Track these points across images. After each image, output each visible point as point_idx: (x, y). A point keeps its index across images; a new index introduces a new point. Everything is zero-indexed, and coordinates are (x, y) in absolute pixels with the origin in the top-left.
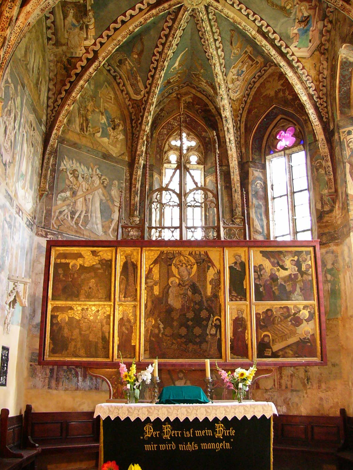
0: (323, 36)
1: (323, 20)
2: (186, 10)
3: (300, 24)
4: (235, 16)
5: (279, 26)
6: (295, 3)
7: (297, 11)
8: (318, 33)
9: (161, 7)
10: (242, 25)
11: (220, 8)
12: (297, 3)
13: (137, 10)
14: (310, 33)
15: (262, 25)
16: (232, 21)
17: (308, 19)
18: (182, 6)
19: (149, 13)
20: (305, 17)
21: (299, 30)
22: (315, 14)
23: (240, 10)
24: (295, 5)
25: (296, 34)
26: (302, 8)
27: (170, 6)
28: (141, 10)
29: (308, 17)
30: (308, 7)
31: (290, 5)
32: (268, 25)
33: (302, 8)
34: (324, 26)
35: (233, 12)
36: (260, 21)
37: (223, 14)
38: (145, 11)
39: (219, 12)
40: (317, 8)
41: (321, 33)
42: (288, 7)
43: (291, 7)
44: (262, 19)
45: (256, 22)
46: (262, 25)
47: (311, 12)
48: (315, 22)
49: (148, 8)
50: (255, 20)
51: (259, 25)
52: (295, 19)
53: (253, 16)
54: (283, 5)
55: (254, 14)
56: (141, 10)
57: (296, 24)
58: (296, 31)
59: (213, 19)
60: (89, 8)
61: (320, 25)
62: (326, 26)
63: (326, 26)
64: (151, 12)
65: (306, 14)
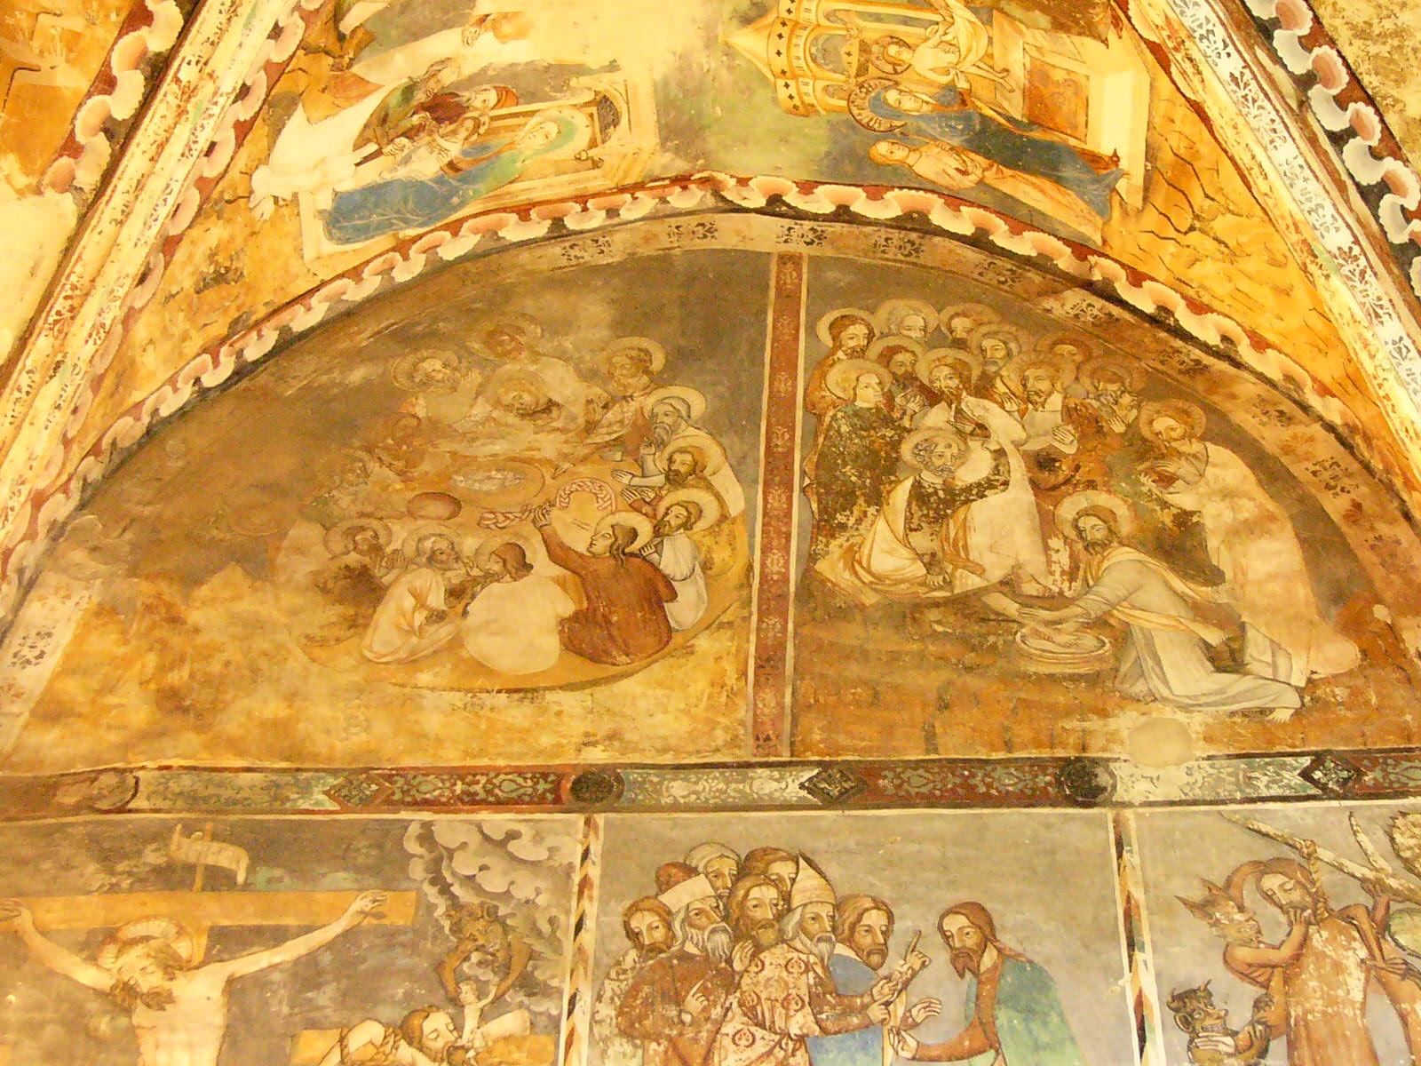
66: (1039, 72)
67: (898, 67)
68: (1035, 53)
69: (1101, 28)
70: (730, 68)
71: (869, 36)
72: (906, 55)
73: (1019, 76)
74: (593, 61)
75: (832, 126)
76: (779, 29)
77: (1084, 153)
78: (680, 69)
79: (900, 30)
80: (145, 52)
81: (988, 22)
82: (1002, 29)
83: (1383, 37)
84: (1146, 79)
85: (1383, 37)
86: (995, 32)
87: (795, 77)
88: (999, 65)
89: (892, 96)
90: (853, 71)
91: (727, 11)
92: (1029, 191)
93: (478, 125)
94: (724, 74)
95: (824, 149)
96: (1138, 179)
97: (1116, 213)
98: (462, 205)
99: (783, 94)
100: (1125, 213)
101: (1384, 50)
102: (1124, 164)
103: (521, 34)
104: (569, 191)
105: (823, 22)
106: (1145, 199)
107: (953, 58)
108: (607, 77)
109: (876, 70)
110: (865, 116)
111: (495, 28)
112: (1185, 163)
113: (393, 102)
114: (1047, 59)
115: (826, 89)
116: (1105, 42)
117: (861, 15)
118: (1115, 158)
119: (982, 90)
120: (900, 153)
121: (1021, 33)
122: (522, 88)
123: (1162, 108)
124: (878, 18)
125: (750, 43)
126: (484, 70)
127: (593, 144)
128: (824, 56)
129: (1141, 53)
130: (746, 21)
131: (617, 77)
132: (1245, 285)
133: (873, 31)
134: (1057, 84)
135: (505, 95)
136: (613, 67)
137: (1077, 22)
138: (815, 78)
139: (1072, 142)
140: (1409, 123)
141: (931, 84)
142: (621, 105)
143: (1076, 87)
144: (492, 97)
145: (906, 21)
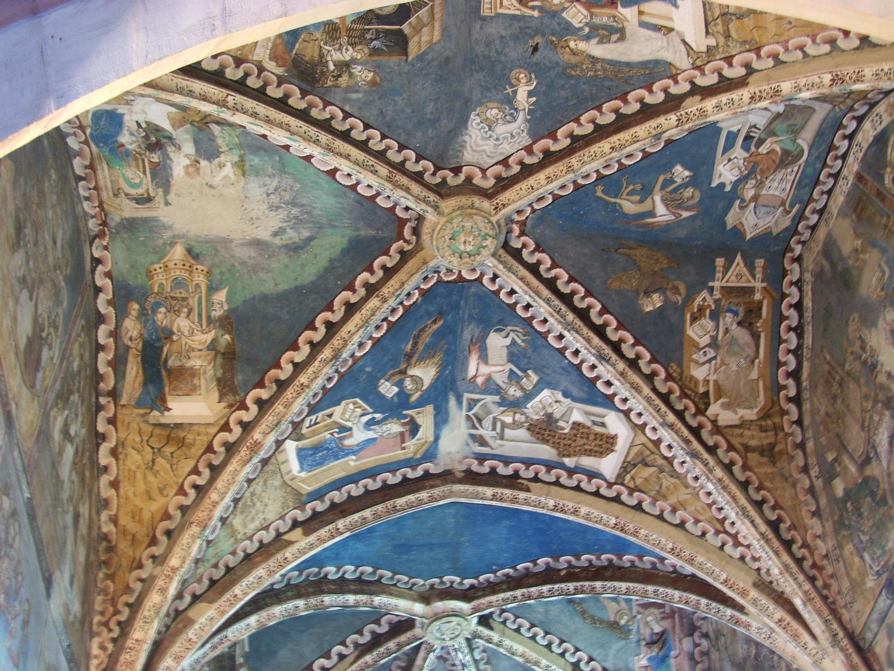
0: (697, 663)
1: (691, 635)
2: (431, 649)
3: (650, 648)
4: (527, 650)
5: (611, 658)
6: (635, 612)
7: (641, 626)
8: (687, 659)
9: (382, 649)
10: (542, 665)
11: (496, 637)
12: (639, 613)
13: (335, 658)
14: (672, 661)
15: (579, 661)
16: (520, 660)
17: (663, 638)
18: (421, 644)
19: (359, 662)
20: (657, 634)
21: (650, 659)
22: (674, 628)
23: (533, 638)
24: (635, 617)
25: (646, 667)
26: (649, 619)
27: (400, 646)
28: (342, 657)
29: (663, 633)
30: (659, 617)
31: (626, 618)
32: (591, 659)
33: (649, 619)
34: (696, 645)
35: (520, 643)
36: (574, 653)
37: (501, 650)
38: (351, 659)
39: (496, 648)
40: (676, 616)
41: (691, 657)
42: (623, 622)
43: (628, 621)
44: (577, 650)
45: (567, 655)
46: (579, 661)
47: (667, 624)
48: (677, 640)
49: (356, 653)
50: (565, 651)
51: (574, 660)
52: (638, 641)
53: (560, 645)
54: (612, 618)
55: (562, 641)
56: (342, 657)
57: (643, 649)
58: (644, 662)
59: (482, 659)
60: (240, 660)
61: (687, 644)
62: (699, 645)
63: (699, 645)
64: (362, 660)
65: (657, 629)
66: (193, 373)
67: (178, 312)
68: (202, 371)
69: (225, 399)
70: (164, 244)
71: (191, 301)
72: (183, 315)
73: (189, 364)
74: (171, 197)
75: (144, 287)
76: (188, 265)
77: (164, 394)
78: (164, 226)
79: (196, 312)
80: (226, 67)
81: (208, 349)
82: (209, 355)
83: (252, 500)
84: (212, 421)
85: (252, 500)
86: (205, 352)
87: (165, 271)
88: (192, 354)
89: (163, 310)
90: (173, 294)
91: (193, 243)
92: (133, 370)
93: (141, 155)
94: (161, 242)
95: (131, 283)
96: (163, 421)
97: (141, 411)
98: (98, 146)
99: (157, 266)
100: (143, 415)
101: (249, 503)
102: (166, 413)
103: (187, 173)
104: (102, 183)
105: (194, 283)
106: (155, 425)
107: (186, 333)
108: (162, 201)
109: (175, 305)
110: (151, 300)
111: (191, 165)
112: (182, 443)
113: (166, 134)
114: (202, 376)
115: (162, 284)
116: (220, 402)
117: (200, 298)
118: (169, 410)
119: (175, 347)
120: (134, 313)
121: (209, 364)
122: (161, 175)
123: (202, 429)
124: (200, 304)
125: (179, 252)
126: (171, 159)
127: (127, 195)
128: (178, 283)
129: (222, 418)
130: (189, 251)
131: (162, 205)
132: (139, 476)
133: (194, 302)
134: (192, 381)
135: (155, 166)
136: (167, 204)
137: (224, 388)
138: (166, 279)
139: (167, 389)
140: (231, 523)
141: (172, 325)
142: (147, 205)
143: (193, 390)
144: (156, 160)
145: (200, 315)
